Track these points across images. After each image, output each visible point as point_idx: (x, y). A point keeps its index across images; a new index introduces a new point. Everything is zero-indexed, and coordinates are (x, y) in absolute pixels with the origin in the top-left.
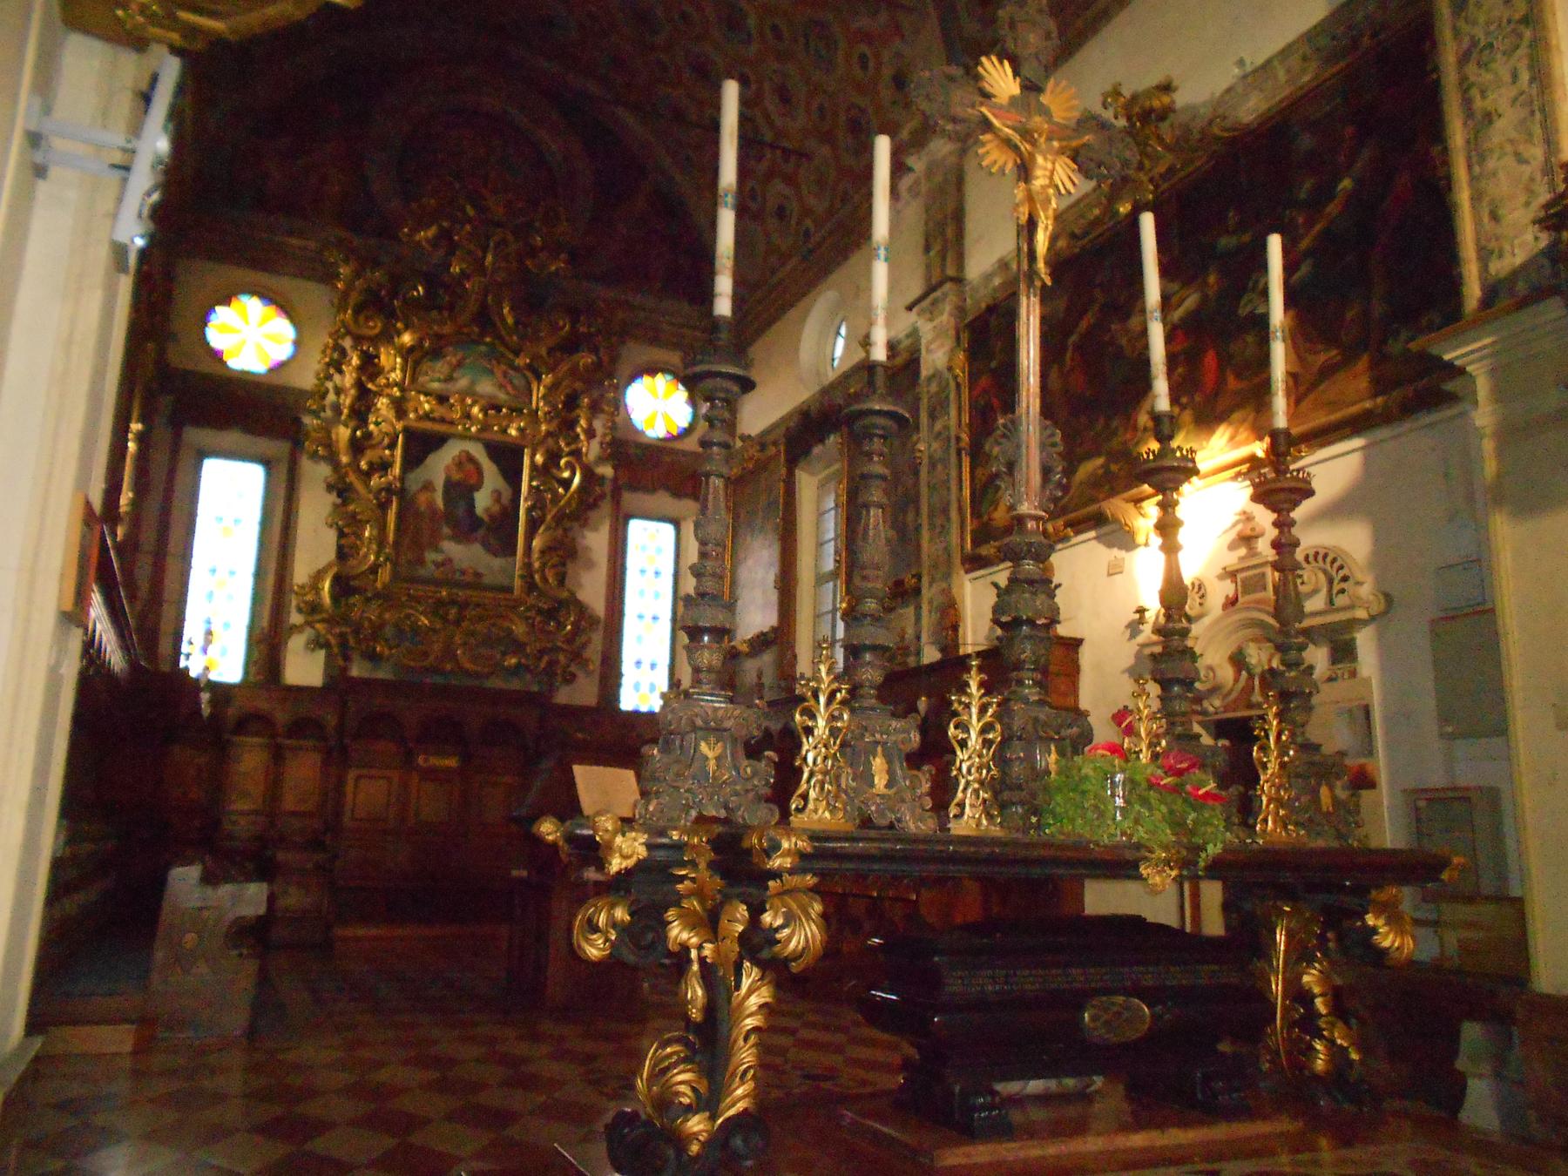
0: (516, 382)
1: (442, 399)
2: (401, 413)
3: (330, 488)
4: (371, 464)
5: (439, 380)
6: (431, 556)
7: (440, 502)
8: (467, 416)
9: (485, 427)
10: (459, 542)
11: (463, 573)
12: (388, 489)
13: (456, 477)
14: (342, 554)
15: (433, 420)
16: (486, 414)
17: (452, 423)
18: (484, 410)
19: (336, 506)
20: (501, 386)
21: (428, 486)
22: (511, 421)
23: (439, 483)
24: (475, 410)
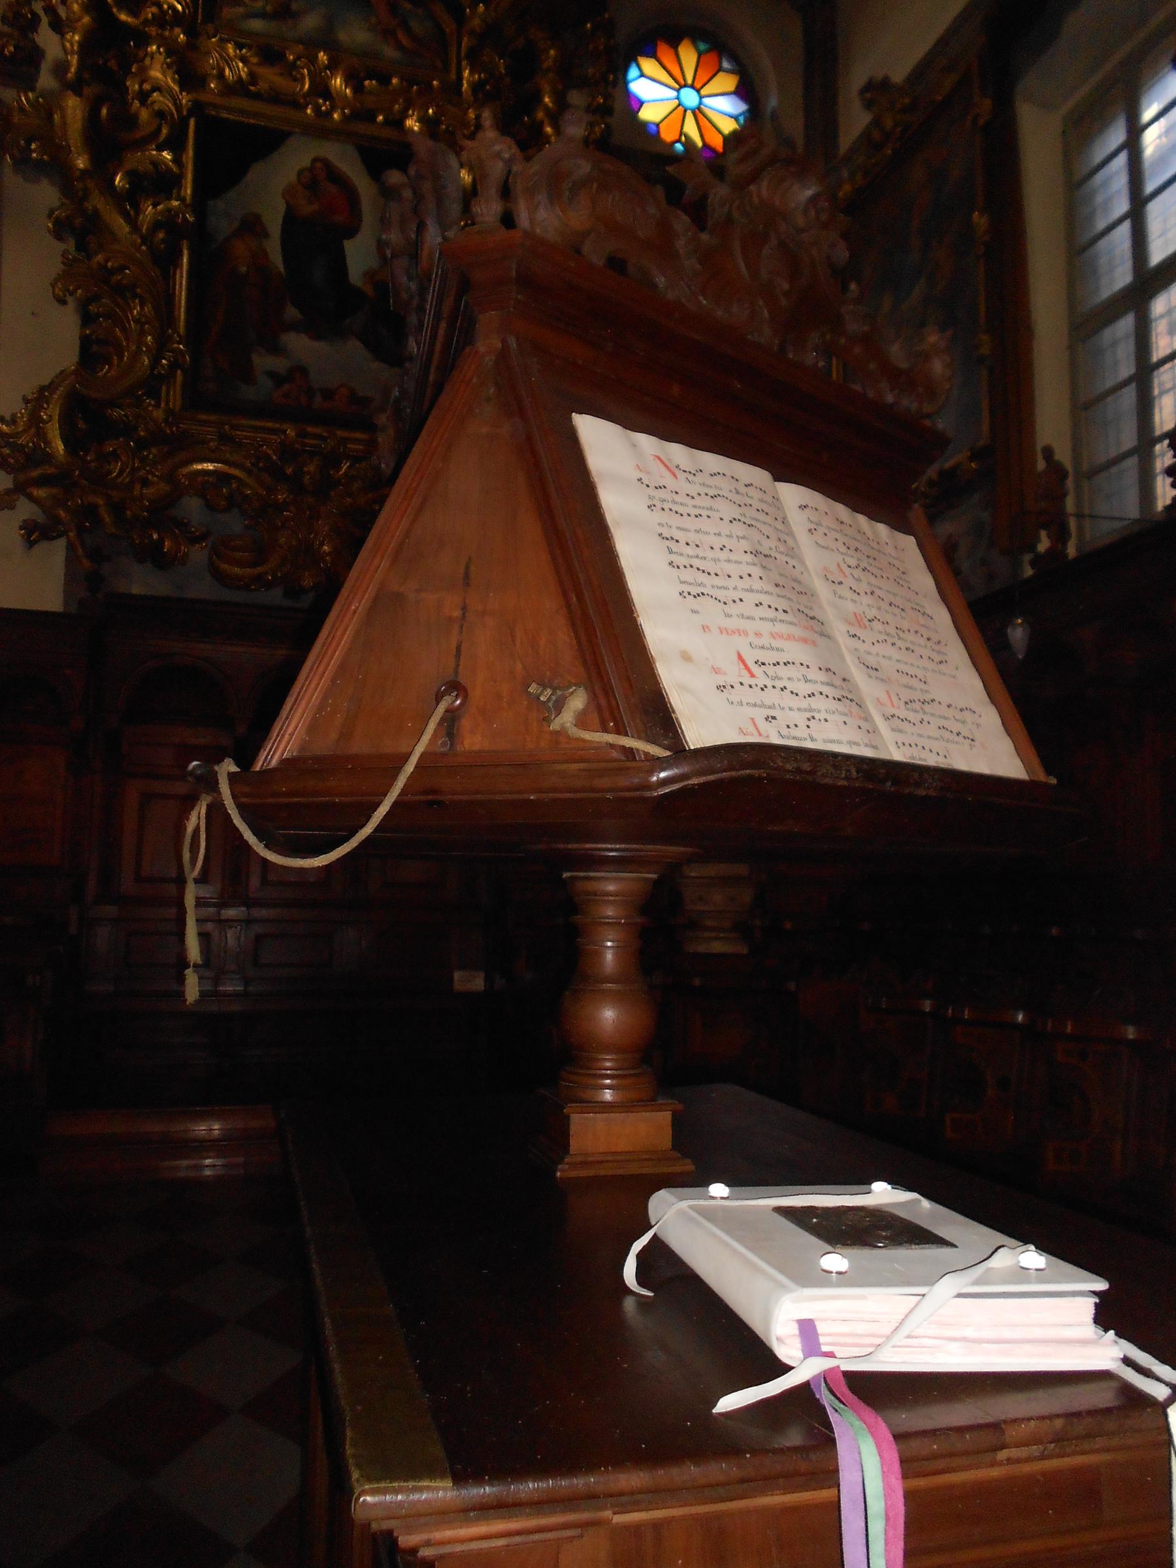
0: (414, 25)
1: (270, 55)
2: (190, 78)
3: (61, 229)
4: (131, 175)
5: (262, 15)
6: (263, 362)
7: (277, 258)
8: (322, 90)
9: (362, 115)
10: (316, 336)
11: (328, 394)
12: (167, 222)
13: (307, 208)
14: (91, 354)
15: (257, 96)
16: (358, 89)
17: (297, 105)
18: (352, 79)
19: (69, 263)
20: (388, 34)
21: (252, 226)
22: (409, 104)
23: (274, 222)
24: (338, 82)
